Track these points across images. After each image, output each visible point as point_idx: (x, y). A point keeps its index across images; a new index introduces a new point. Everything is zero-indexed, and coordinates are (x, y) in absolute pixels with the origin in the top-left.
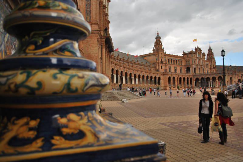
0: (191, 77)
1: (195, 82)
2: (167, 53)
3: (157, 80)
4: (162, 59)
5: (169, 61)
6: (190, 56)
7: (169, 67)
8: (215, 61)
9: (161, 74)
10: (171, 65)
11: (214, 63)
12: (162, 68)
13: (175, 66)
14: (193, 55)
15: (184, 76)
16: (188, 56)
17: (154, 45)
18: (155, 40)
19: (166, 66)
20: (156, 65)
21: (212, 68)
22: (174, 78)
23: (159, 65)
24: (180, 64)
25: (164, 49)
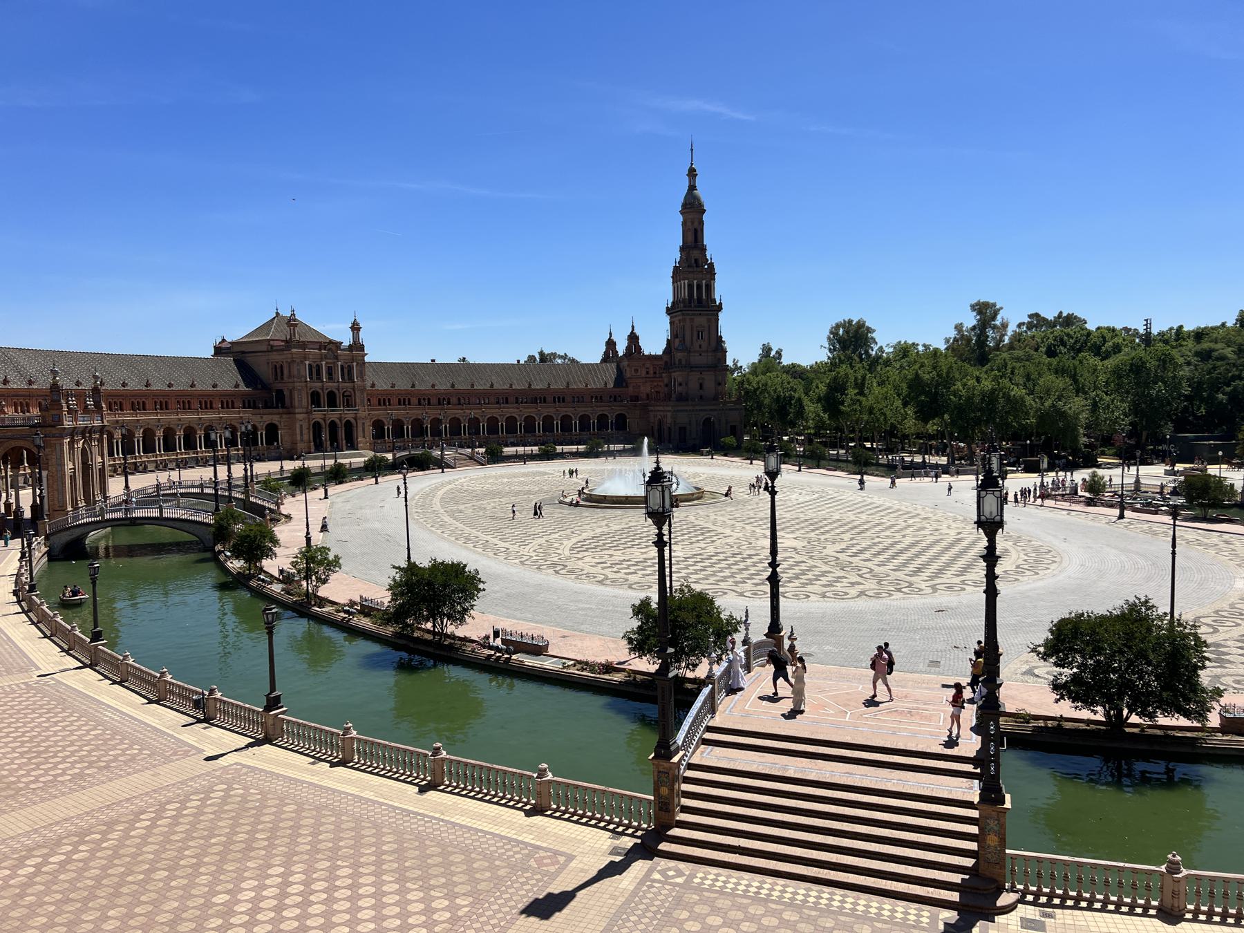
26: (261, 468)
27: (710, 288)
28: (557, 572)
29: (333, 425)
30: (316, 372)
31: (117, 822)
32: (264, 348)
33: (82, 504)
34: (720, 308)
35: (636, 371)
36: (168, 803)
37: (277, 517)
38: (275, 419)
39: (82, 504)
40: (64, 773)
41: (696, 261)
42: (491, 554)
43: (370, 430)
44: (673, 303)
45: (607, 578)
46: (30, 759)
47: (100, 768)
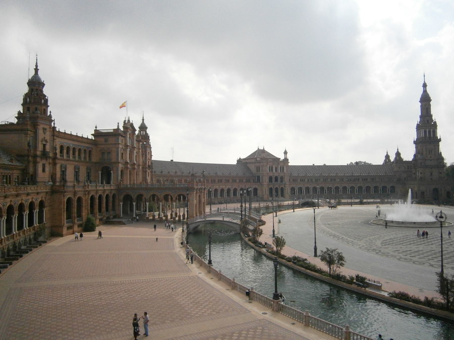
0: (113, 192)
1: (121, 203)
2: (57, 130)
3: (36, 211)
4: (44, 145)
5: (61, 152)
6: (111, 140)
7: (61, 166)
8: (151, 152)
9: (47, 193)
10: (68, 162)
11: (150, 156)
12: (44, 171)
13: (76, 163)
14: (120, 138)
15: (100, 193)
16: (106, 141)
17: (22, 102)
18: (26, 89)
19: (55, 164)
20: (29, 162)
21: (146, 168)
22: (79, 200)
23: (35, 163)
24: (88, 160)
25: (53, 119)
26: (255, 205)
27: (435, 132)
28: (377, 253)
29: (277, 189)
30: (271, 169)
31: (226, 335)
32: (253, 161)
33: (198, 214)
34: (440, 140)
35: (399, 168)
36: (242, 331)
37: (263, 223)
38: (257, 187)
39: (198, 214)
40: (205, 312)
41: (428, 121)
42: (346, 243)
43: (289, 191)
44: (417, 139)
45: (401, 258)
46: (194, 305)
47: (216, 312)
